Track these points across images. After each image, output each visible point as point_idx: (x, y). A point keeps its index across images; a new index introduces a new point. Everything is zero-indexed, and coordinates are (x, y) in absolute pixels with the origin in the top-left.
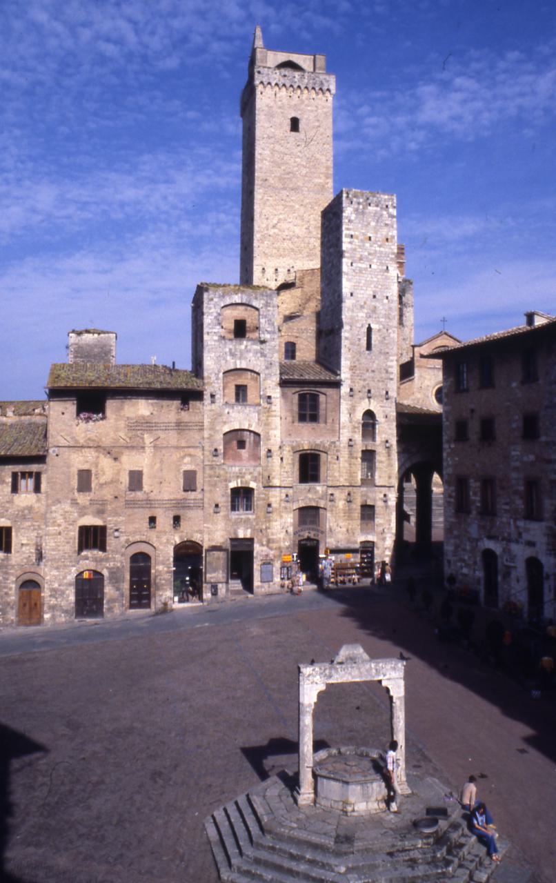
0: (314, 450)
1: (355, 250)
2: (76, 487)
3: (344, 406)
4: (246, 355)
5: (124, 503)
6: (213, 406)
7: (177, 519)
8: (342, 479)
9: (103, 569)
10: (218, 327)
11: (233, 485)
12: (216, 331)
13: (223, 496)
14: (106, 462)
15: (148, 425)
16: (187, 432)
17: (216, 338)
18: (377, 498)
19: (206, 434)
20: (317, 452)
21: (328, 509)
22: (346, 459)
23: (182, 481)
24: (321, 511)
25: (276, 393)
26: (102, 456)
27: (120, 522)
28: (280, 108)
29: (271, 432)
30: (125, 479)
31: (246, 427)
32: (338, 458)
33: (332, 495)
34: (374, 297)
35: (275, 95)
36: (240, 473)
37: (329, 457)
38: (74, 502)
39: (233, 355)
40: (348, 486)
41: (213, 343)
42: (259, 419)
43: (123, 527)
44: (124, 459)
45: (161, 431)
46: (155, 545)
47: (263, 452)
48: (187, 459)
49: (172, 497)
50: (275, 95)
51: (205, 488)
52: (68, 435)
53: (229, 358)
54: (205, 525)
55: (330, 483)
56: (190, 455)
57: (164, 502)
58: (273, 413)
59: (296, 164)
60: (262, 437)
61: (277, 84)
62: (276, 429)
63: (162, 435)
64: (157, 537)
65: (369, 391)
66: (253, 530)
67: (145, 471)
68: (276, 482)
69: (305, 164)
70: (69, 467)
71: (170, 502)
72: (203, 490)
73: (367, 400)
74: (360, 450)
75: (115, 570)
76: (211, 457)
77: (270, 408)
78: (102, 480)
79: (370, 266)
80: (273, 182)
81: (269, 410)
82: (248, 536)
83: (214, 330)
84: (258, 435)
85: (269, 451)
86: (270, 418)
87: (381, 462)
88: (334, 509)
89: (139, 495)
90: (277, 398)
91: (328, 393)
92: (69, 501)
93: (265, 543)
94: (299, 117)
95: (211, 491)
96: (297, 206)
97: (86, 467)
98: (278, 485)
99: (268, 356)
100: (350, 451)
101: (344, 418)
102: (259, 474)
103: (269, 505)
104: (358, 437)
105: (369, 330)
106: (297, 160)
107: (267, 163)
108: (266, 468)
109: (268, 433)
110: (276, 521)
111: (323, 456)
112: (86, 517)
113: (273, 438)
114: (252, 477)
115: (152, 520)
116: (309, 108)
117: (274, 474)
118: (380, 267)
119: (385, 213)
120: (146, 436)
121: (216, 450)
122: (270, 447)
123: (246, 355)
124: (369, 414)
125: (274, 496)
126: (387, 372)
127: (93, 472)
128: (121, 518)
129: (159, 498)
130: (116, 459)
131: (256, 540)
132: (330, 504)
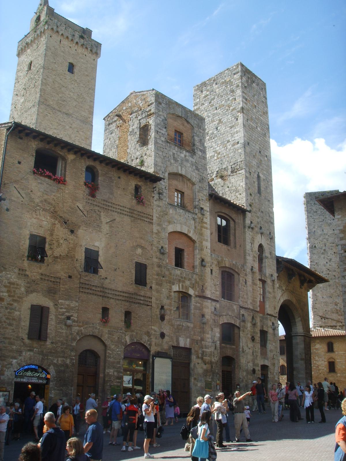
0: (232, 269)
1: (248, 110)
2: (26, 254)
3: (249, 234)
4: (185, 163)
5: (78, 285)
6: (161, 203)
7: (128, 314)
8: (249, 303)
9: (49, 365)
10: (165, 130)
11: (176, 288)
12: (164, 133)
13: (168, 297)
14: (61, 232)
15: (105, 203)
16: (139, 221)
17: (163, 139)
18: (269, 326)
19: (155, 228)
20: (232, 271)
21: (241, 329)
22: (251, 284)
23: (134, 272)
24: (236, 331)
25: (207, 206)
26: (58, 226)
27: (72, 309)
28: (63, 52)
29: (204, 243)
30: (81, 256)
31: (186, 233)
32: (246, 283)
33: (243, 315)
34: (260, 152)
35: (60, 42)
36: (182, 277)
37: (241, 279)
38: (22, 273)
39: (176, 160)
40: (252, 310)
41: (161, 143)
42: (195, 227)
43: (76, 315)
44: (80, 232)
45: (116, 213)
46: (106, 342)
47: (197, 262)
48: (139, 251)
49: (125, 289)
50: (60, 42)
51: (154, 286)
52: (23, 189)
53: (172, 161)
54: (153, 327)
55: (241, 303)
56: (142, 248)
57: (117, 293)
58: (205, 225)
59: (69, 96)
60: (197, 245)
61: (62, 35)
62: (207, 241)
63: (116, 216)
64: (110, 333)
65: (261, 228)
66: (193, 341)
67: (101, 253)
68: (208, 294)
69: (75, 98)
70: (20, 228)
71: (122, 294)
72: (151, 287)
73: (260, 235)
74: (258, 278)
75: (62, 368)
76: (158, 254)
77: (202, 219)
78: (57, 253)
79: (257, 127)
80: (52, 103)
81: (202, 222)
82: (188, 346)
83: (162, 132)
84: (194, 241)
85: (203, 260)
86: (203, 229)
87: (270, 293)
88: (245, 330)
89: (94, 280)
90: (208, 212)
91: (236, 221)
92: (16, 270)
93: (200, 355)
94: (74, 63)
95: (158, 291)
96: (67, 127)
97: (41, 232)
98: (209, 297)
99: (201, 170)
100: (252, 277)
101: (248, 247)
102: (196, 282)
103: (203, 316)
104: (256, 266)
105: (259, 177)
106: (71, 93)
107: (49, 88)
108: (202, 277)
109: (202, 243)
110: (208, 334)
111: (236, 276)
112: (34, 294)
113: (205, 249)
114: (191, 283)
115: (105, 311)
116: (82, 60)
117: (206, 284)
118: (262, 131)
119: (261, 93)
120: (102, 213)
121: (162, 247)
122: (203, 257)
123: (185, 163)
124: (261, 246)
125: (208, 308)
126: (269, 216)
127: (47, 240)
128: (73, 304)
129: (113, 287)
130: (72, 232)
131: (193, 351)
132: (242, 324)
